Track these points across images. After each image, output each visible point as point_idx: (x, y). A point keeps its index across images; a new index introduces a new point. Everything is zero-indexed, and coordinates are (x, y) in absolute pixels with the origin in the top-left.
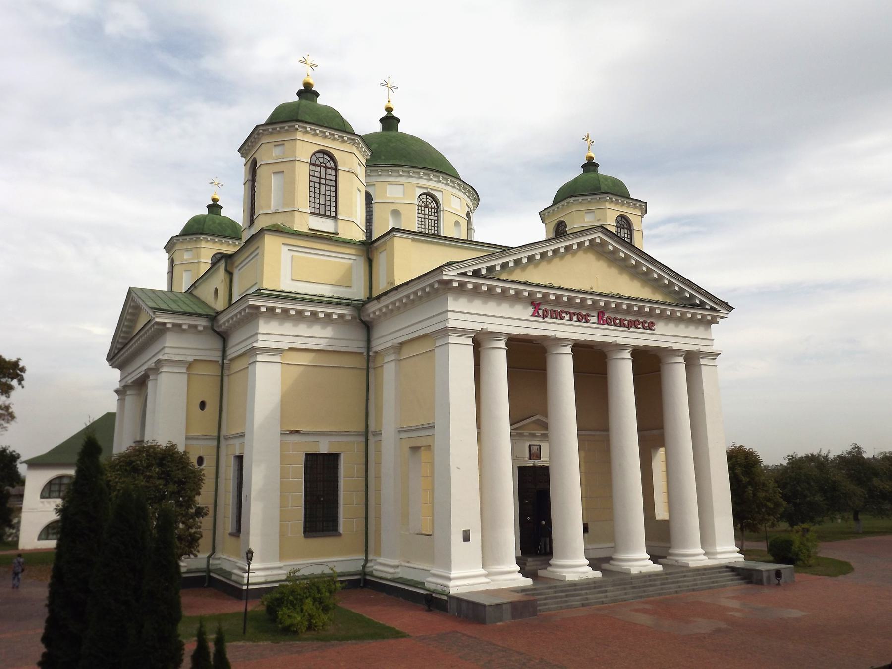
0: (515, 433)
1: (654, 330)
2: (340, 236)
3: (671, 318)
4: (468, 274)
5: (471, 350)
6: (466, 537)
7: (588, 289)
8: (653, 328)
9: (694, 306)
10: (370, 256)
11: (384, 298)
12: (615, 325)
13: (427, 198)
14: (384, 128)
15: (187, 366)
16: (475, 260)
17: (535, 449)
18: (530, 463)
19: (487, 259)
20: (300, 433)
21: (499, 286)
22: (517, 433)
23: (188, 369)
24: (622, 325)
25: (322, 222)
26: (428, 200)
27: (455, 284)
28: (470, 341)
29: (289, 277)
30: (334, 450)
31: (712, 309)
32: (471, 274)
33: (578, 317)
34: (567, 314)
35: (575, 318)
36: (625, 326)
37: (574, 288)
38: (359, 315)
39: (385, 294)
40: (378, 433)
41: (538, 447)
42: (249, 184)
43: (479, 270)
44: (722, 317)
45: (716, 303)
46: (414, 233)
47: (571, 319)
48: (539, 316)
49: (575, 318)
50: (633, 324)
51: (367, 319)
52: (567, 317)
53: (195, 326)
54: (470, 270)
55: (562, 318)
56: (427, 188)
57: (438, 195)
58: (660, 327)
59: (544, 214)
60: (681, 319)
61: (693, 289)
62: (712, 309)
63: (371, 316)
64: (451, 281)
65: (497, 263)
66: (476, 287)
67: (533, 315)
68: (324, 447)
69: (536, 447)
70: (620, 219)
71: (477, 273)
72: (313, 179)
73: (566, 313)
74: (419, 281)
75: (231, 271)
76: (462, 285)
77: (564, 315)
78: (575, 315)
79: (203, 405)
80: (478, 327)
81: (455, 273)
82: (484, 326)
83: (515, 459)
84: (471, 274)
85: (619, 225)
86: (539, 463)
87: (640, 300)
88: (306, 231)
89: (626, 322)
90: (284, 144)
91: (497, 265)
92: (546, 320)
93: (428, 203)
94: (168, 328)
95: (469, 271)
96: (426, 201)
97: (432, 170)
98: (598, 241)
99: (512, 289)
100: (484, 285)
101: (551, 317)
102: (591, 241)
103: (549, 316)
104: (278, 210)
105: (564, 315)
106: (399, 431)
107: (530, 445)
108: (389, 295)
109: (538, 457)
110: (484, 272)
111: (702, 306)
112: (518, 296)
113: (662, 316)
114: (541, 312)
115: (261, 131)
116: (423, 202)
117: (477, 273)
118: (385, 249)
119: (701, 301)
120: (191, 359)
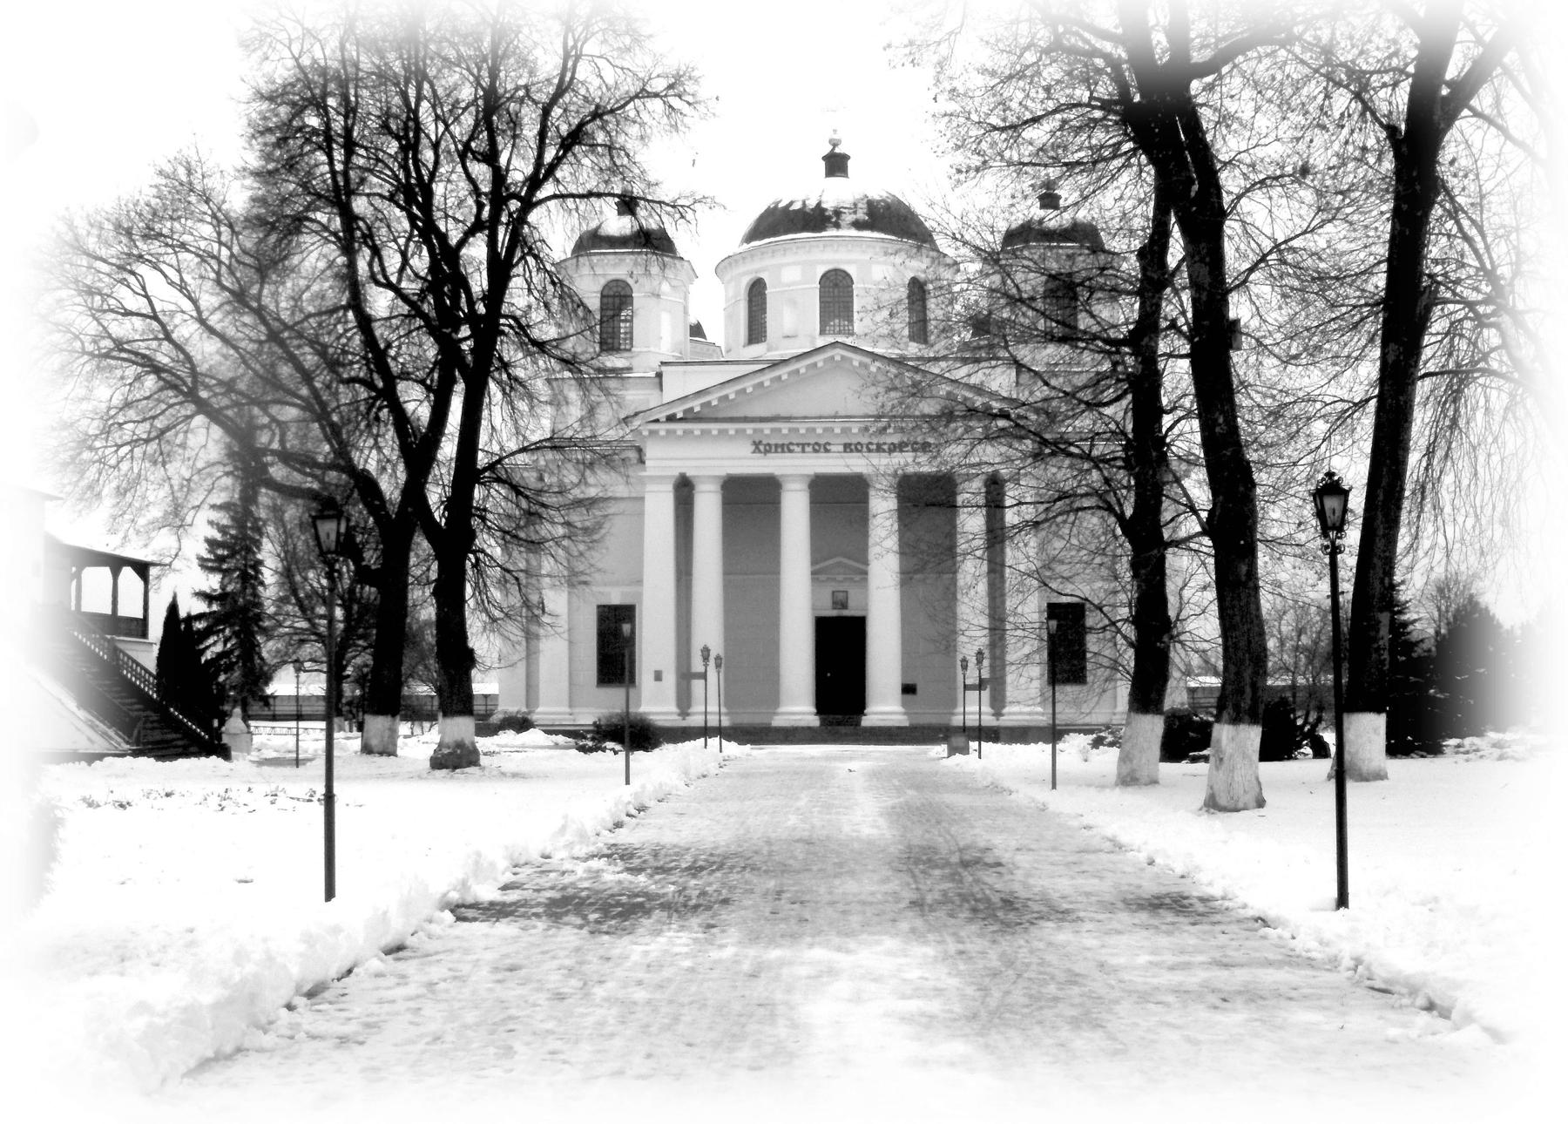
6: (658, 676)
17: (841, 596)
18: (834, 613)
30: (627, 601)
35: (808, 449)
36: (884, 451)
47: (803, 451)
48: (760, 452)
52: (799, 449)
54: (662, 416)
55: (790, 451)
71: (671, 419)
73: (798, 445)
82: (683, 471)
83: (814, 608)
86: (846, 613)
89: (886, 447)
98: (838, 358)
100: (679, 428)
101: (776, 452)
109: (844, 606)
114: (762, 448)
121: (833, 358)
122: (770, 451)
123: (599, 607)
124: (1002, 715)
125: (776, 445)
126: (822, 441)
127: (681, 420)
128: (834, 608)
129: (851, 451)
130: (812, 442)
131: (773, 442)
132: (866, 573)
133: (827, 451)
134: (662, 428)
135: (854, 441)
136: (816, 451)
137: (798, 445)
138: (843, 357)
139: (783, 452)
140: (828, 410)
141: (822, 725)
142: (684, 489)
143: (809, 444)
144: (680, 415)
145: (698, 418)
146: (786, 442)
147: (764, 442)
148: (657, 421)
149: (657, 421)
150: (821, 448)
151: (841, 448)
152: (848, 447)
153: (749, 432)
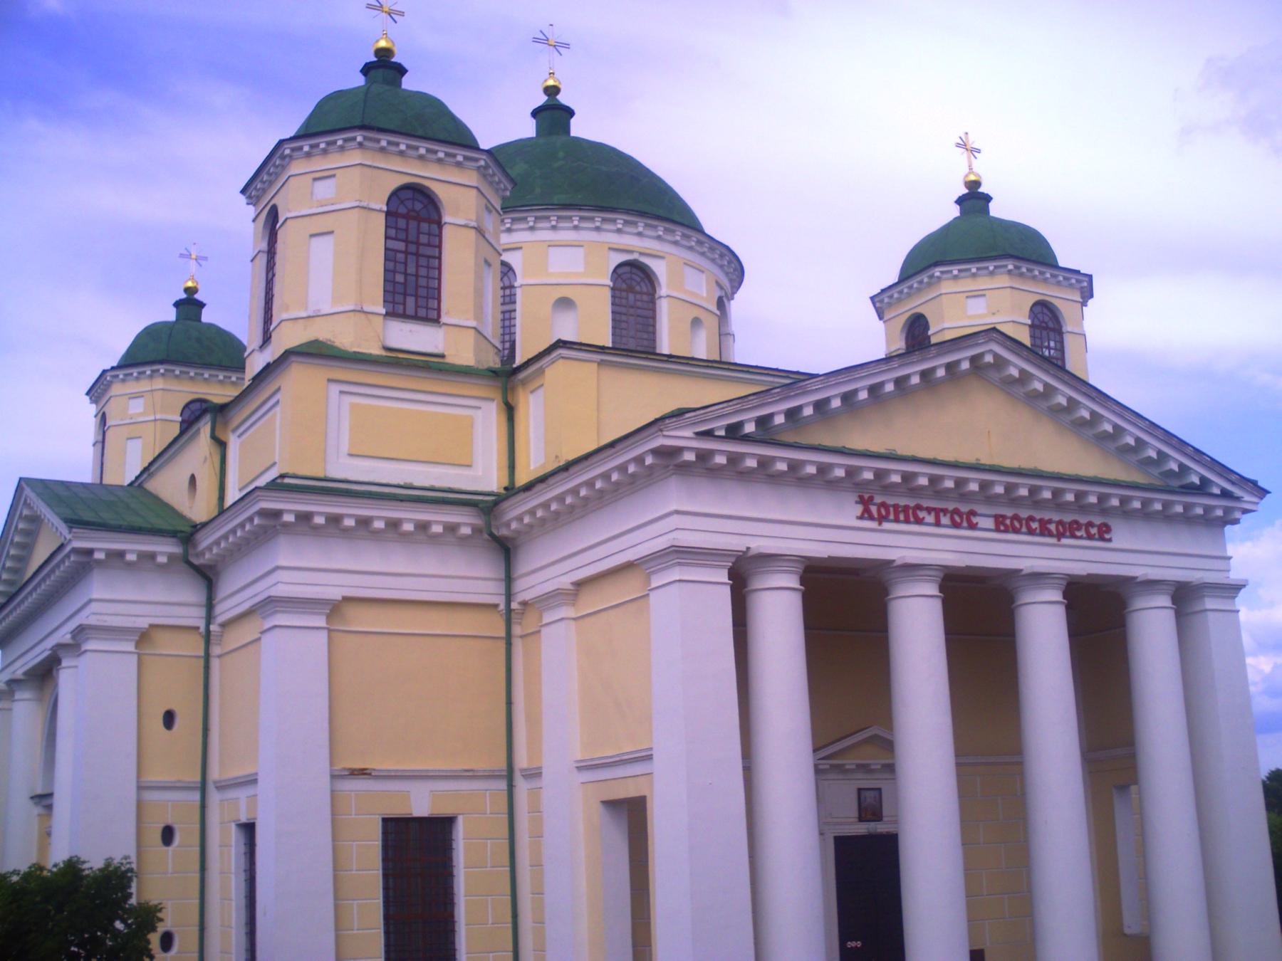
0: (828, 767)
1: (1110, 540)
3: (1145, 515)
4: (717, 433)
5: (725, 593)
7: (968, 458)
8: (1107, 536)
9: (1190, 489)
10: (510, 401)
11: (540, 487)
12: (1031, 532)
15: (137, 638)
16: (731, 404)
17: (869, 797)
18: (862, 829)
20: (370, 774)
21: (781, 458)
22: (832, 766)
23: (138, 644)
24: (1044, 531)
25: (411, 331)
26: (634, 276)
27: (690, 457)
28: (723, 576)
29: (345, 448)
30: (444, 810)
31: (1225, 494)
32: (722, 433)
33: (952, 519)
34: (929, 513)
35: (945, 520)
36: (1050, 534)
38: (489, 525)
39: (542, 480)
40: (534, 774)
41: (876, 793)
42: (262, 260)
43: (740, 425)
44: (1245, 511)
45: (1233, 483)
46: (602, 349)
48: (871, 518)
49: (945, 520)
50: (1068, 530)
51: (504, 532)
52: (930, 518)
53: (152, 556)
54: (719, 426)
55: (919, 521)
58: (1123, 536)
59: (882, 301)
60: (1166, 517)
61: (1186, 455)
62: (1225, 494)
63: (514, 525)
64: (679, 450)
65: (778, 412)
68: (421, 803)
69: (872, 794)
70: (1038, 309)
71: (734, 432)
72: (392, 244)
73: (929, 510)
74: (613, 450)
75: (222, 438)
77: (921, 514)
78: (945, 515)
79: (169, 719)
80: (738, 544)
81: (688, 433)
84: (722, 433)
85: (1037, 322)
86: (880, 828)
88: (376, 351)
89: (1052, 527)
90: (334, 176)
91: (779, 413)
92: (886, 526)
94: (99, 562)
95: (719, 428)
96: (631, 279)
97: (642, 214)
98: (989, 358)
99: (811, 463)
100: (751, 455)
101: (897, 520)
102: (974, 360)
103: (892, 517)
104: (319, 311)
105: (921, 514)
106: (577, 767)
107: (860, 790)
108: (551, 481)
113: (1125, 512)
114: (874, 509)
115: (287, 152)
117: (734, 432)
118: (542, 385)
120: (144, 623)
123: (385, 821)
125: (896, 507)
127: (747, 439)
128: (861, 819)
136: (956, 525)
137: (929, 510)
139: (907, 521)
140: (967, 457)
143: (945, 511)
146: (912, 503)
147: (878, 500)
148: (708, 434)
149: (708, 434)
150: (964, 520)
152: (1001, 524)
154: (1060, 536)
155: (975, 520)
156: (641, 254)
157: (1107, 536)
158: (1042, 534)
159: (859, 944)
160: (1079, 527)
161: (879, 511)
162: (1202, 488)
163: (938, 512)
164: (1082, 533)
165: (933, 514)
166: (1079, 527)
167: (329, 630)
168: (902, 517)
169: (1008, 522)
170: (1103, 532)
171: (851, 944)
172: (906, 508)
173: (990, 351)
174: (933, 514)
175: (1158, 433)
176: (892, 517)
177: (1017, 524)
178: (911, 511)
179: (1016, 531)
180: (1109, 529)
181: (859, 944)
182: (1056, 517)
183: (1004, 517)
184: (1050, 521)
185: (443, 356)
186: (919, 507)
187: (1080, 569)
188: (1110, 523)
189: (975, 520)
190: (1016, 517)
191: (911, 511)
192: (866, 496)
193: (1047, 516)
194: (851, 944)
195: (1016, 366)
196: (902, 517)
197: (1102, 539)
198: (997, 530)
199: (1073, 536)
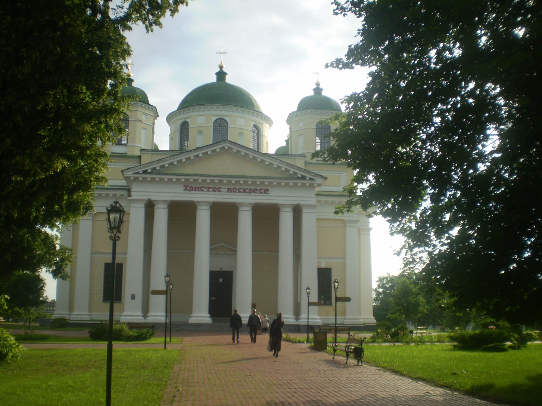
1: (268, 193)
2: (128, 155)
4: (140, 173)
6: (133, 297)
9: (299, 178)
12: (240, 192)
13: (217, 122)
14: (218, 79)
19: (150, 164)
24: (244, 191)
31: (311, 179)
32: (142, 172)
33: (213, 190)
35: (210, 190)
36: (247, 192)
37: (212, 174)
43: (147, 170)
45: (314, 176)
47: (208, 191)
48: (187, 190)
52: (206, 190)
54: (141, 171)
55: (202, 191)
56: (219, 116)
57: (227, 119)
62: (311, 179)
66: (144, 179)
67: (184, 190)
71: (145, 172)
73: (206, 188)
76: (136, 179)
77: (203, 189)
80: (146, 198)
81: (131, 173)
82: (149, 197)
84: (142, 172)
87: (252, 177)
89: (247, 191)
93: (221, 124)
98: (226, 148)
100: (149, 177)
101: (195, 190)
105: (203, 189)
110: (149, 171)
111: (303, 178)
112: (178, 180)
114: (188, 188)
116: (223, 124)
117: (145, 172)
119: (302, 175)
121: (224, 147)
122: (192, 190)
124: (299, 319)
125: (195, 187)
126: (217, 187)
127: (150, 173)
129: (231, 192)
130: (213, 187)
131: (194, 186)
132: (236, 251)
133: (220, 191)
134: (141, 177)
135: (232, 187)
136: (214, 191)
137: (206, 188)
138: (229, 147)
139: (198, 191)
141: (213, 322)
142: (150, 206)
143: (211, 188)
144: (149, 171)
145: (158, 173)
146: (200, 186)
147: (190, 186)
148: (138, 173)
149: (138, 173)
150: (216, 189)
151: (226, 190)
152: (229, 190)
153: (183, 180)
154: (249, 193)
155: (220, 190)
156: (222, 116)
157: (267, 192)
158: (244, 192)
159: (215, 298)
160: (257, 190)
161: (190, 189)
162: (303, 178)
163: (208, 188)
164: (258, 192)
165: (207, 189)
166: (257, 190)
167: (93, 220)
168: (197, 190)
169: (232, 190)
170: (266, 191)
171: (212, 298)
172: (199, 187)
173: (226, 146)
174: (207, 189)
175: (284, 163)
176: (194, 189)
177: (235, 190)
178: (200, 189)
179: (235, 192)
180: (268, 190)
181: (215, 298)
182: (249, 188)
183: (231, 189)
184: (247, 189)
185: (126, 154)
186: (203, 187)
187: (254, 201)
188: (268, 189)
189: (220, 190)
190: (235, 188)
191: (200, 189)
192: (186, 185)
193: (245, 188)
194: (212, 298)
195: (235, 149)
196: (197, 190)
197: (265, 193)
198: (228, 192)
199: (255, 193)
